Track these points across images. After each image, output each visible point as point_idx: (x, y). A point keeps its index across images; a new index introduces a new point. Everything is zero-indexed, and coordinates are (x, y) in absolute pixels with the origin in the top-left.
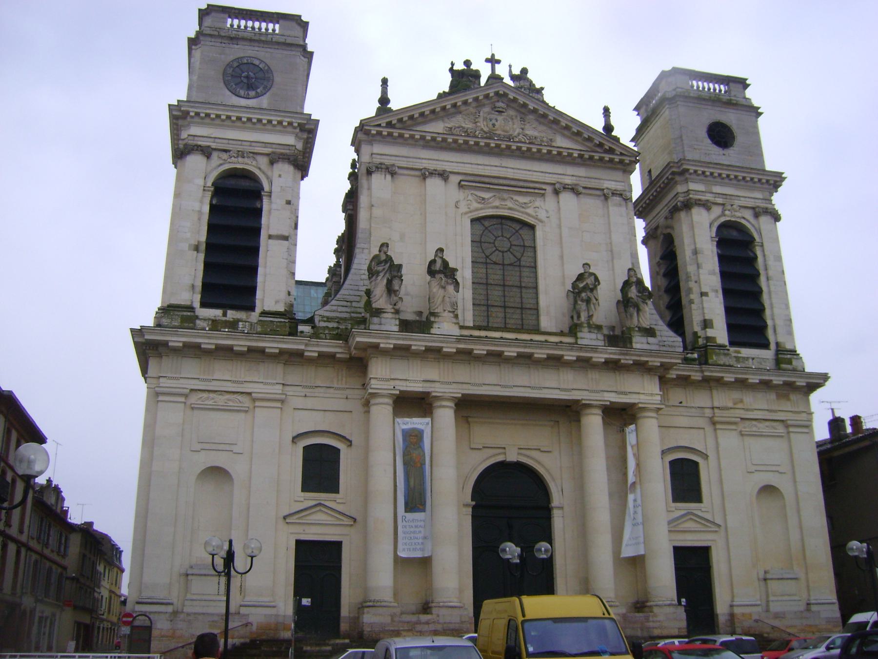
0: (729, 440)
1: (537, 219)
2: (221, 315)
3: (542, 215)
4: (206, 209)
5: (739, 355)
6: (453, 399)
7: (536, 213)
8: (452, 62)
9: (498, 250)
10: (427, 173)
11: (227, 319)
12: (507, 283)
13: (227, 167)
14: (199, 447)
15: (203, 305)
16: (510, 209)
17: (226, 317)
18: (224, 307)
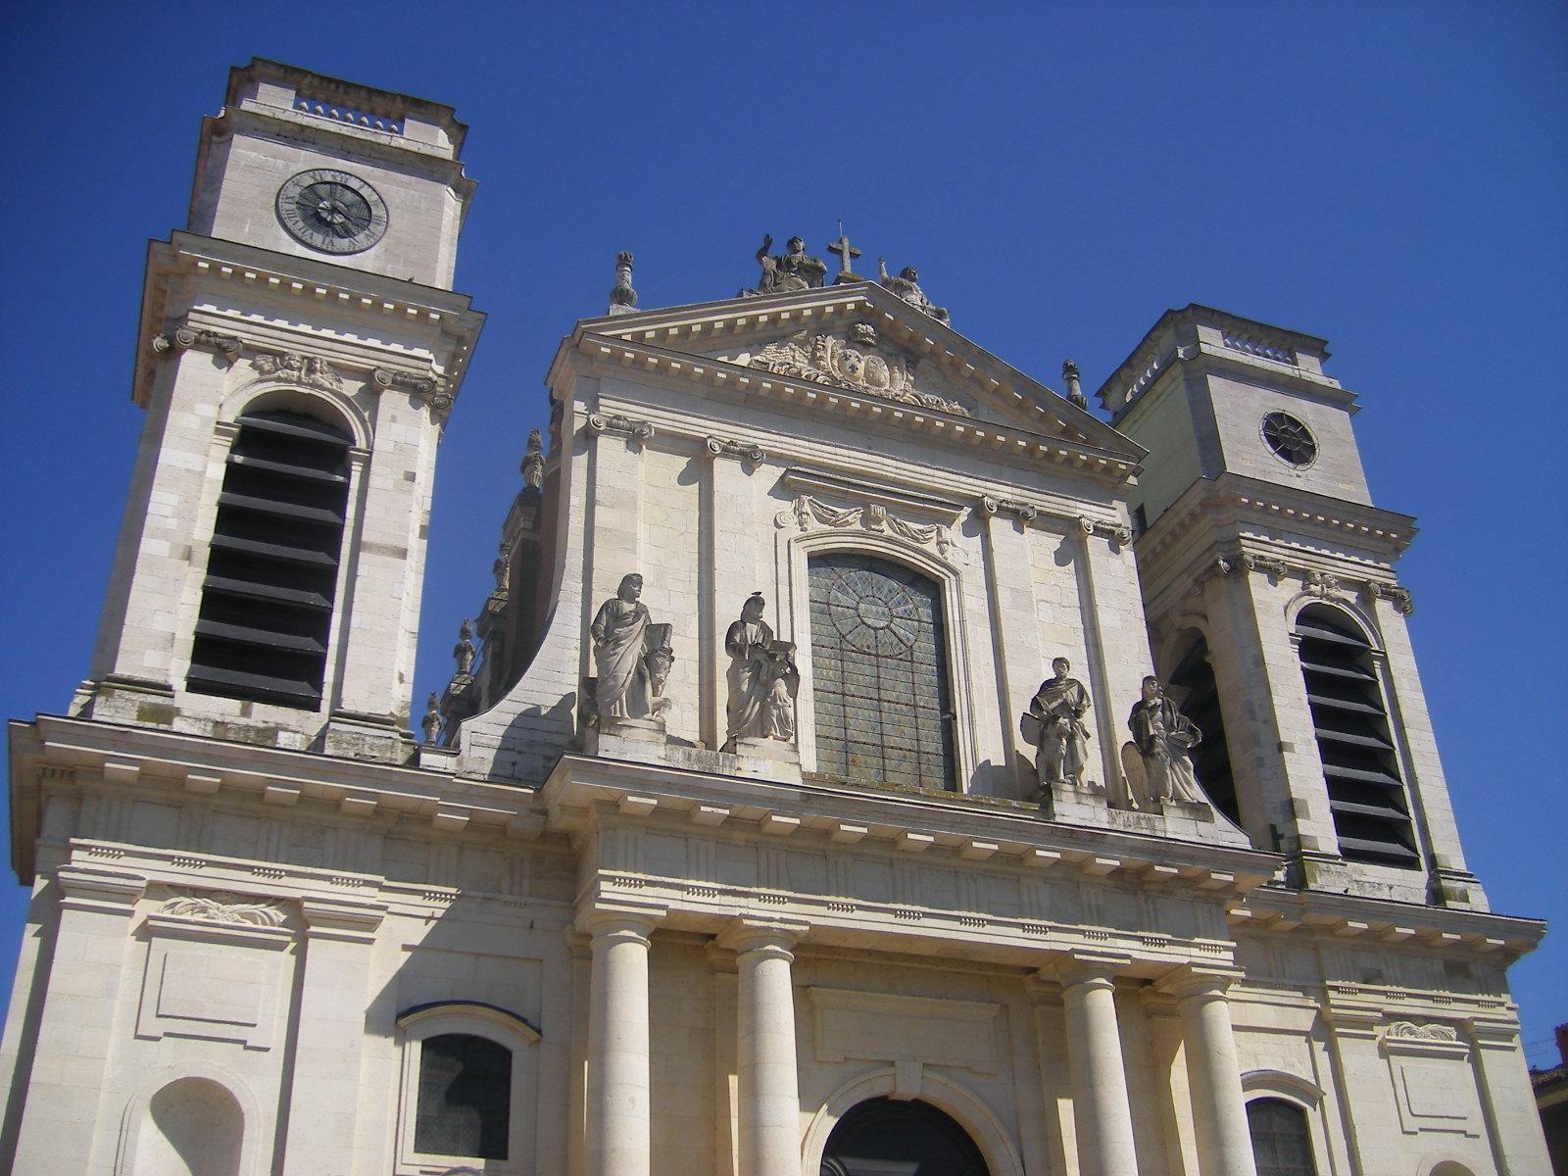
0: (1358, 1056)
2: (237, 712)
3: (953, 557)
4: (217, 472)
5: (1364, 879)
8: (768, 236)
9: (865, 624)
10: (718, 450)
11: (251, 722)
12: (884, 695)
13: (271, 387)
14: (156, 1027)
15: (195, 686)
16: (889, 540)
17: (249, 717)
18: (247, 695)
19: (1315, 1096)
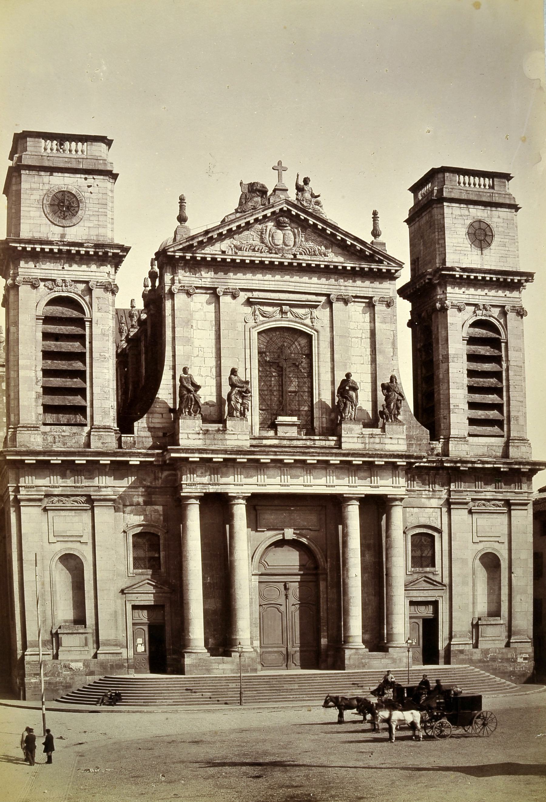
1: (312, 329)
3: (317, 326)
6: (244, 498)
7: (312, 323)
19: (439, 531)
